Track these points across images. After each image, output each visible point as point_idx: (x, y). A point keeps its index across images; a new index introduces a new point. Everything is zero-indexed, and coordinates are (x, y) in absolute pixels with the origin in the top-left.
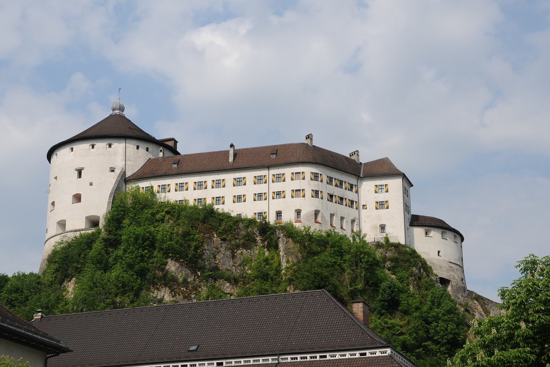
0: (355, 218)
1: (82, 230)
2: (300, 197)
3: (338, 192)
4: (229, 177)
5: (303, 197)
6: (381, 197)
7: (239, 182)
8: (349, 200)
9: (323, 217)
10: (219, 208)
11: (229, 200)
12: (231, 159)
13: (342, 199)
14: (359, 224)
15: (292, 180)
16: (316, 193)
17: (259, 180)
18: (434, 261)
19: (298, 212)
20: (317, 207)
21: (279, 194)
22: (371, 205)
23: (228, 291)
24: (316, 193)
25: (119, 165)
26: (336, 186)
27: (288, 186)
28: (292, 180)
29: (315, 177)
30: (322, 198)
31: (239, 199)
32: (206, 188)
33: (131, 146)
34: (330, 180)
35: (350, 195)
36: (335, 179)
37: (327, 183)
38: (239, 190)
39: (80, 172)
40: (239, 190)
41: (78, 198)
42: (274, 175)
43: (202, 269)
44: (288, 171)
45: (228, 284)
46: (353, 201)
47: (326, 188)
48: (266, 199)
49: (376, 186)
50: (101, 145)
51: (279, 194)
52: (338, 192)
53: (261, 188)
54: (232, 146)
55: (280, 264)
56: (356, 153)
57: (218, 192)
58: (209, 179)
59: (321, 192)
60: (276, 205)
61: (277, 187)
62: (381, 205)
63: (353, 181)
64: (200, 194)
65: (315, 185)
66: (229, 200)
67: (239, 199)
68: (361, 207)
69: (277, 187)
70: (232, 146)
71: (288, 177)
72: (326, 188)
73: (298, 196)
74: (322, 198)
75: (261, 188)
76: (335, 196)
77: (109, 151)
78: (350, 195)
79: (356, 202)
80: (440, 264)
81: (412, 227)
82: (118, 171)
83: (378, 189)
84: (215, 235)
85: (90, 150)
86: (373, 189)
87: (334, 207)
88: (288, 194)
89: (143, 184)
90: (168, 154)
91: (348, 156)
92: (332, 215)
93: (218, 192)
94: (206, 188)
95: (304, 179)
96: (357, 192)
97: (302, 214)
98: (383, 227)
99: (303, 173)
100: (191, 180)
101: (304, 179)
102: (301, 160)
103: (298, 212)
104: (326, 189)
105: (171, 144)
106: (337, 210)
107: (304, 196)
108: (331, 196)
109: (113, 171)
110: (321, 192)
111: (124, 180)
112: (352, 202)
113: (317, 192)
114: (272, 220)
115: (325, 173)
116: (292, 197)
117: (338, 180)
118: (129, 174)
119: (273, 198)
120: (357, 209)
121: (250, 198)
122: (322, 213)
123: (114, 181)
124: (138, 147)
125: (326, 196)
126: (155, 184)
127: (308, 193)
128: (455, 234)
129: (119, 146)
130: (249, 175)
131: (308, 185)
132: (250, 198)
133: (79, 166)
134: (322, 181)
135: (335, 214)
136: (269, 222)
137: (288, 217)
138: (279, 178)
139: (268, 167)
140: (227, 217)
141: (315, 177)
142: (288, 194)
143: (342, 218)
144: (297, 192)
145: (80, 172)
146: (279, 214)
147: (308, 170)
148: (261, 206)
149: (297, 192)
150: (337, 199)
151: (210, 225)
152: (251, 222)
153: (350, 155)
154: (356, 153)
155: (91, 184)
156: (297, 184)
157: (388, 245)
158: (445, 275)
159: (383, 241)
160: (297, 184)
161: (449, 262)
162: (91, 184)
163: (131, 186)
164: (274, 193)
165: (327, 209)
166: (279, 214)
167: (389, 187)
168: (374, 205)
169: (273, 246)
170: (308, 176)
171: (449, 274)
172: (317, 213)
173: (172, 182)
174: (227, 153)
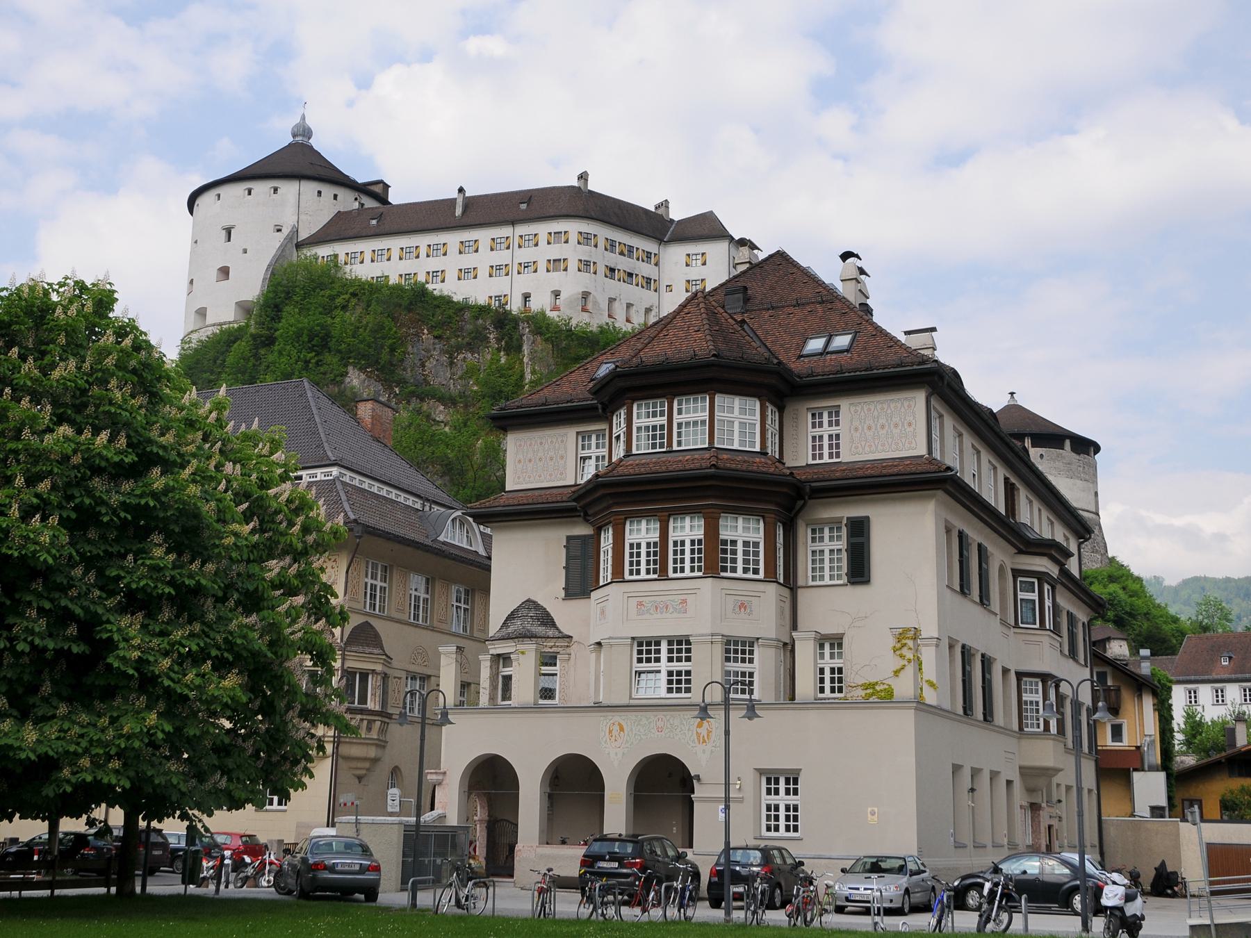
0: (652, 306)
1: (230, 323)
2: (560, 271)
3: (623, 263)
4: (453, 239)
5: (564, 270)
8: (643, 277)
10: (435, 288)
11: (451, 276)
12: (459, 211)
13: (630, 275)
15: (549, 243)
16: (585, 265)
19: (557, 294)
20: (587, 287)
23: (440, 418)
25: (288, 222)
26: (622, 253)
28: (549, 243)
29: (585, 239)
30: (595, 273)
32: (417, 257)
33: (310, 188)
34: (611, 246)
35: (645, 269)
36: (620, 243)
37: (606, 249)
38: (468, 261)
39: (229, 231)
40: (468, 261)
41: (225, 272)
42: (521, 236)
43: (402, 382)
44: (543, 229)
45: (442, 408)
46: (651, 279)
47: (604, 256)
48: (507, 274)
49: (688, 255)
50: (262, 188)
52: (623, 263)
53: (502, 257)
54: (461, 190)
55: (522, 377)
56: (665, 204)
57: (434, 264)
58: (423, 241)
59: (594, 263)
60: (523, 283)
61: (525, 255)
63: (651, 246)
64: (408, 266)
65: (585, 252)
66: (451, 276)
68: (663, 288)
69: (525, 255)
70: (461, 190)
72: (604, 256)
73: (555, 270)
74: (595, 273)
75: (502, 257)
76: (619, 270)
77: (274, 200)
78: (645, 269)
79: (655, 281)
82: (286, 231)
84: (425, 331)
85: (244, 197)
86: (684, 259)
87: (616, 287)
88: (542, 266)
89: (324, 251)
90: (370, 203)
91: (653, 209)
92: (612, 300)
93: (434, 264)
94: (417, 257)
95: (566, 242)
96: (656, 264)
97: (563, 296)
99: (565, 232)
101: (566, 242)
102: (564, 212)
103: (557, 294)
104: (604, 258)
105: (378, 189)
107: (566, 270)
108: (612, 270)
109: (279, 230)
110: (594, 263)
112: (648, 280)
113: (587, 263)
114: (515, 306)
115: (604, 232)
116: (548, 271)
117: (625, 245)
118: (303, 235)
119: (519, 273)
120: (656, 291)
121: (483, 272)
122: (594, 297)
124: (335, 197)
125: (601, 269)
126: (341, 250)
127: (573, 265)
129: (289, 189)
130: (484, 236)
131: (573, 252)
132: (483, 272)
133: (227, 224)
134: (596, 246)
135: (618, 299)
136: (511, 310)
137: (540, 302)
139: (513, 223)
140: (446, 301)
143: (629, 306)
144: (556, 264)
145: (229, 231)
146: (526, 297)
147: (573, 227)
151: (418, 314)
152: (483, 310)
153: (656, 208)
154: (665, 204)
155: (245, 251)
156: (556, 251)
160: (556, 251)
162: (245, 251)
163: (308, 252)
164: (520, 264)
166: (526, 297)
167: (708, 257)
169: (513, 348)
170: (573, 238)
172: (585, 295)
173: (366, 246)
174: (453, 201)
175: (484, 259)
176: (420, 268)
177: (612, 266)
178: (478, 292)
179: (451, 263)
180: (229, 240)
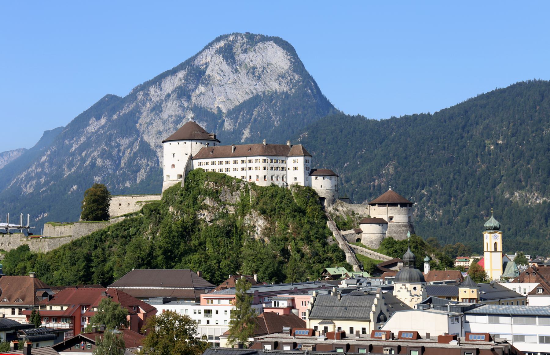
4: (231, 160)
6: (295, 165)
7: (235, 162)
9: (268, 178)
10: (228, 174)
13: (277, 168)
14: (286, 178)
17: (243, 162)
18: (319, 190)
21: (250, 169)
22: (292, 169)
24: (265, 168)
26: (275, 163)
27: (253, 165)
29: (265, 161)
31: (235, 169)
33: (194, 143)
35: (282, 165)
40: (235, 166)
41: (173, 166)
50: (181, 143)
51: (250, 169)
53: (244, 165)
57: (227, 166)
58: (224, 160)
60: (249, 173)
61: (250, 165)
62: (296, 169)
63: (284, 158)
65: (265, 165)
66: (231, 169)
67: (235, 169)
69: (250, 165)
71: (254, 161)
75: (244, 165)
78: (282, 165)
81: (310, 176)
82: (189, 155)
83: (295, 161)
88: (254, 168)
93: (227, 166)
96: (285, 163)
98: (296, 178)
100: (217, 160)
111: (191, 158)
112: (283, 168)
121: (239, 169)
123: (187, 159)
126: (203, 161)
127: (262, 168)
129: (189, 143)
130: (239, 159)
132: (239, 169)
133: (174, 152)
137: (254, 179)
138: (250, 161)
141: (265, 161)
142: (254, 168)
143: (277, 177)
146: (250, 177)
147: (262, 158)
148: (243, 173)
149: (256, 168)
150: (275, 168)
155: (178, 160)
156: (257, 165)
157: (297, 186)
158: (323, 196)
159: (295, 184)
160: (257, 165)
162: (178, 160)
166: (250, 177)
168: (293, 168)
170: (261, 161)
173: (210, 161)
175: (239, 166)
176: (224, 167)
178: (238, 175)
179: (231, 166)
180: (174, 157)
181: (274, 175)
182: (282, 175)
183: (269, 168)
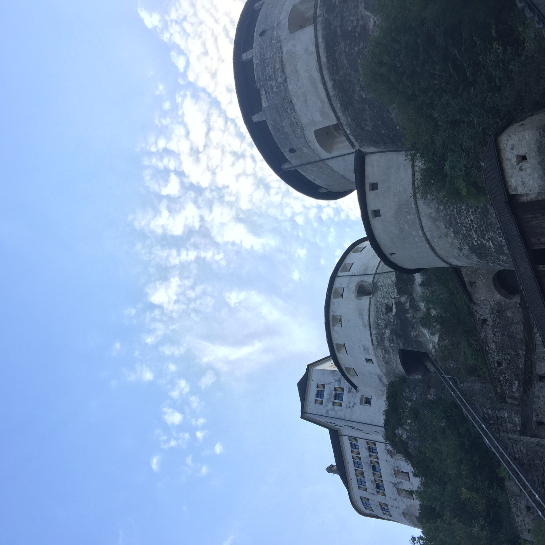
8: (370, 456)
13: (374, 468)
18: (384, 370)
36: (357, 475)
47: (372, 494)
72: (372, 494)
78: (364, 453)
80: (383, 363)
87: (388, 488)
106: (390, 483)
108: (378, 486)
113: (383, 509)
117: (356, 470)
128: (331, 323)
161: (373, 344)
165: (396, 499)
171: (391, 351)
177: (375, 486)
181: (395, 485)
182: (389, 457)
183: (380, 498)
